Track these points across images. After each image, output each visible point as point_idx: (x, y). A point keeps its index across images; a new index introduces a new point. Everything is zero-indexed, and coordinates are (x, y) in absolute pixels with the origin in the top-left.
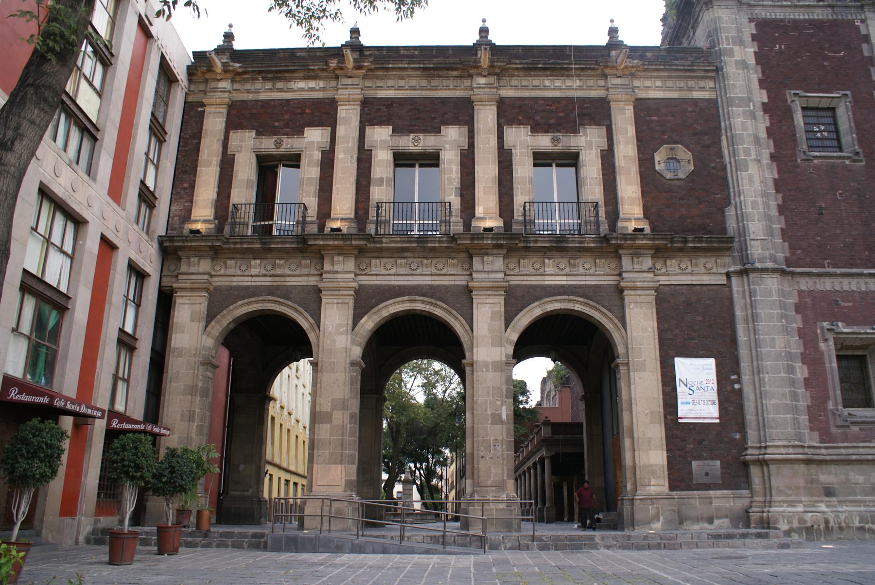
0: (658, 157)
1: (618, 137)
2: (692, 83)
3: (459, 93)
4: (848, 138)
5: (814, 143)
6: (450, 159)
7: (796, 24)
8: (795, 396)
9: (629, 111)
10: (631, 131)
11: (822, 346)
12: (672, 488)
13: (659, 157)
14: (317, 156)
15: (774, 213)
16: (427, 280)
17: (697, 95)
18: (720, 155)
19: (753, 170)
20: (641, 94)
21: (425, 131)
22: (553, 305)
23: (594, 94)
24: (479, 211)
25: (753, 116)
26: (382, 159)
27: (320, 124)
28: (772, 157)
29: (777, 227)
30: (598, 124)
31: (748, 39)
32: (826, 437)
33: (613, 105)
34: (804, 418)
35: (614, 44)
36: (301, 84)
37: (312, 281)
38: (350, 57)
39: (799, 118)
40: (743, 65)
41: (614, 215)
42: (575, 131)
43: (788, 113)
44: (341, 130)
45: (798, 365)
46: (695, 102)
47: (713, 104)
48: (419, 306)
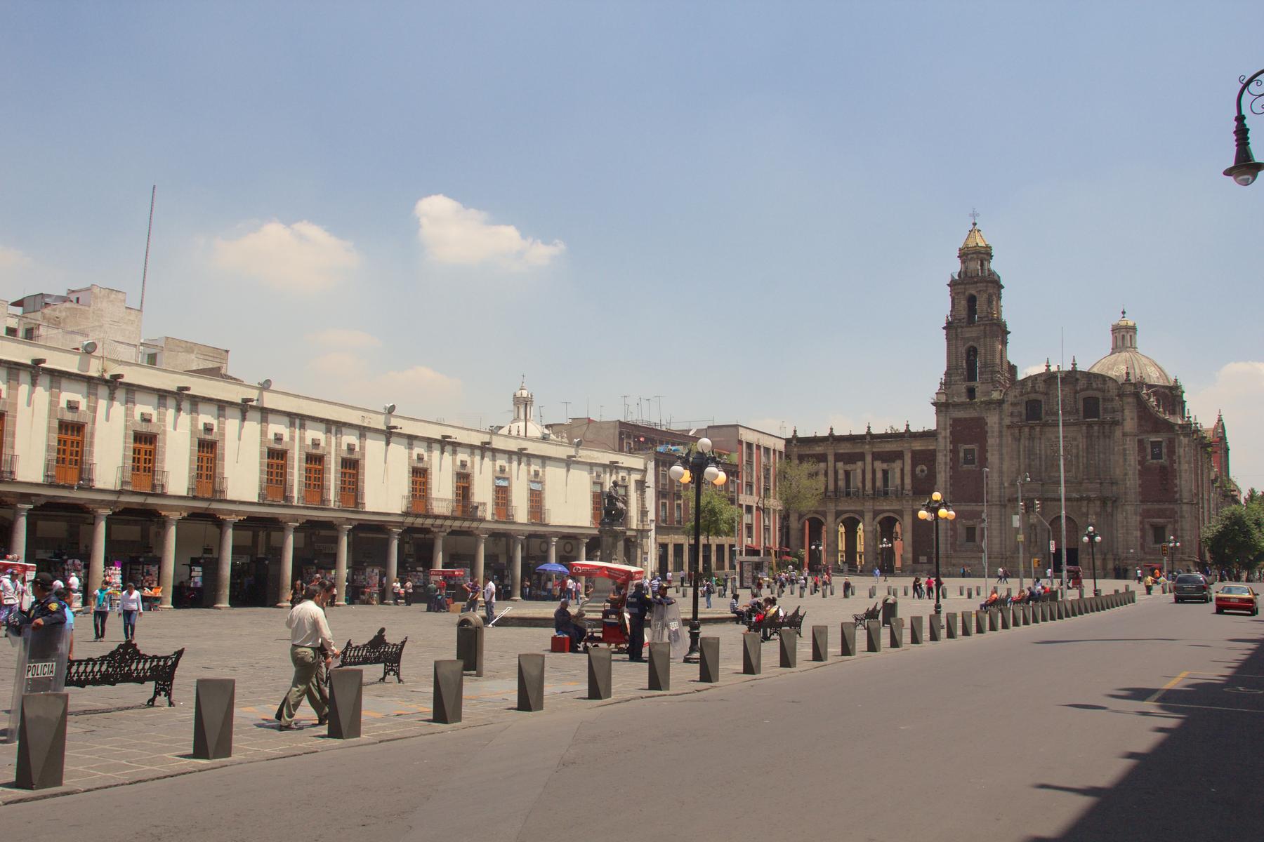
0: (917, 469)
1: (905, 464)
2: (929, 444)
3: (861, 450)
4: (976, 460)
5: (967, 462)
6: (859, 472)
7: (965, 419)
8: (947, 540)
9: (910, 455)
10: (910, 462)
11: (958, 526)
12: (913, 563)
13: (918, 469)
14: (823, 472)
15: (948, 487)
16: (853, 508)
17: (931, 448)
18: (935, 468)
19: (943, 474)
20: (914, 449)
21: (852, 463)
22: (886, 515)
23: (900, 449)
24: (867, 488)
25: (946, 456)
26: (841, 472)
27: (824, 462)
28: (951, 468)
29: (949, 491)
30: (900, 459)
31: (948, 426)
32: (955, 551)
33: (905, 453)
34: (949, 546)
35: (908, 430)
36: (817, 449)
37: (825, 509)
38: (831, 439)
39: (962, 455)
40: (945, 438)
41: (903, 488)
42: (894, 462)
43: (958, 452)
44: (829, 464)
45: (949, 532)
46: (929, 450)
47: (935, 450)
48: (852, 515)
